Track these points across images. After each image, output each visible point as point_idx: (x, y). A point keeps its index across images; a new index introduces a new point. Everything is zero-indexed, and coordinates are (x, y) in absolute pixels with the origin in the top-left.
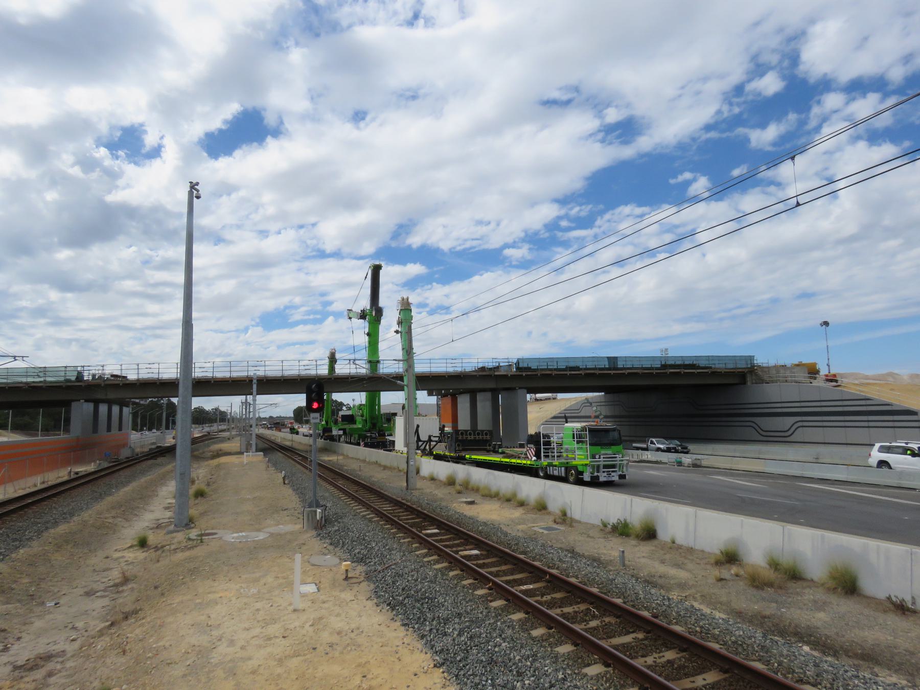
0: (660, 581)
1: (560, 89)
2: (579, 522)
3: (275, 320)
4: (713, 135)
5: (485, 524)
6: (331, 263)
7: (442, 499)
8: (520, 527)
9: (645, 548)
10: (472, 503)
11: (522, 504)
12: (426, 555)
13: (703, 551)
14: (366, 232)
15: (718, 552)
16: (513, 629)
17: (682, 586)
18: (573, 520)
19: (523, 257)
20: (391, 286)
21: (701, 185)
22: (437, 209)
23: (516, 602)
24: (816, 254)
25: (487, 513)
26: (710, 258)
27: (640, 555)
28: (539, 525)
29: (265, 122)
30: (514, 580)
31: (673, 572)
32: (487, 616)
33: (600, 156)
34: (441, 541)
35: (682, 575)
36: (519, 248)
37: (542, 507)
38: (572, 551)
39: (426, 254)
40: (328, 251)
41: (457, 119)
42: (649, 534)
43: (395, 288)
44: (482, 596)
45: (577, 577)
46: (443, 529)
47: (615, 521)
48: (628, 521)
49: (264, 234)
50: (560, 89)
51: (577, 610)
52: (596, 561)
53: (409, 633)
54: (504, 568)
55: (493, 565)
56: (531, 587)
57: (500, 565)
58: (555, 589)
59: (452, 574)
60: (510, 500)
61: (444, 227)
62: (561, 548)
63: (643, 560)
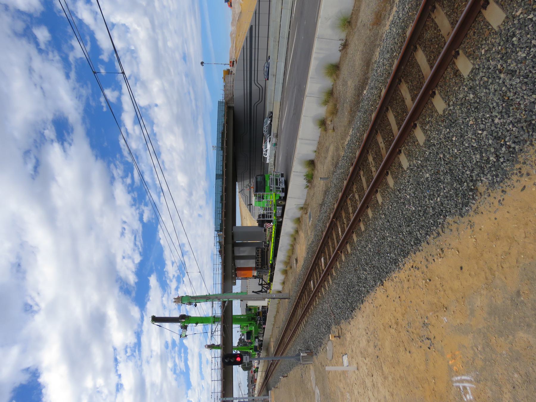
0: (335, 160)
1: (25, 163)
2: (306, 200)
3: (183, 376)
4: (73, 75)
5: (308, 253)
6: (144, 339)
7: (295, 278)
8: (309, 233)
9: (319, 166)
10: (296, 260)
11: (297, 232)
12: (325, 289)
13: (320, 137)
14: (123, 312)
15: (320, 129)
17: (337, 149)
19: (150, 211)
20: (164, 299)
21: (111, 95)
22: (110, 263)
23: (347, 239)
24: (160, 44)
25: (302, 252)
26: (159, 101)
27: (322, 169)
28: (308, 223)
29: (24, 382)
30: (336, 239)
31: (330, 153)
32: (355, 255)
33: (80, 145)
34: (317, 279)
35: (332, 148)
36: (143, 211)
37: (298, 221)
38: (322, 205)
39: (142, 272)
41: (40, 236)
42: (312, 163)
43: (166, 295)
44: (345, 257)
47: (305, 181)
49: (119, 387)
50: (25, 163)
53: (366, 300)
54: (330, 244)
55: (329, 250)
57: (329, 246)
59: (334, 274)
60: (295, 237)
61: (124, 258)
62: (320, 211)
63: (325, 168)
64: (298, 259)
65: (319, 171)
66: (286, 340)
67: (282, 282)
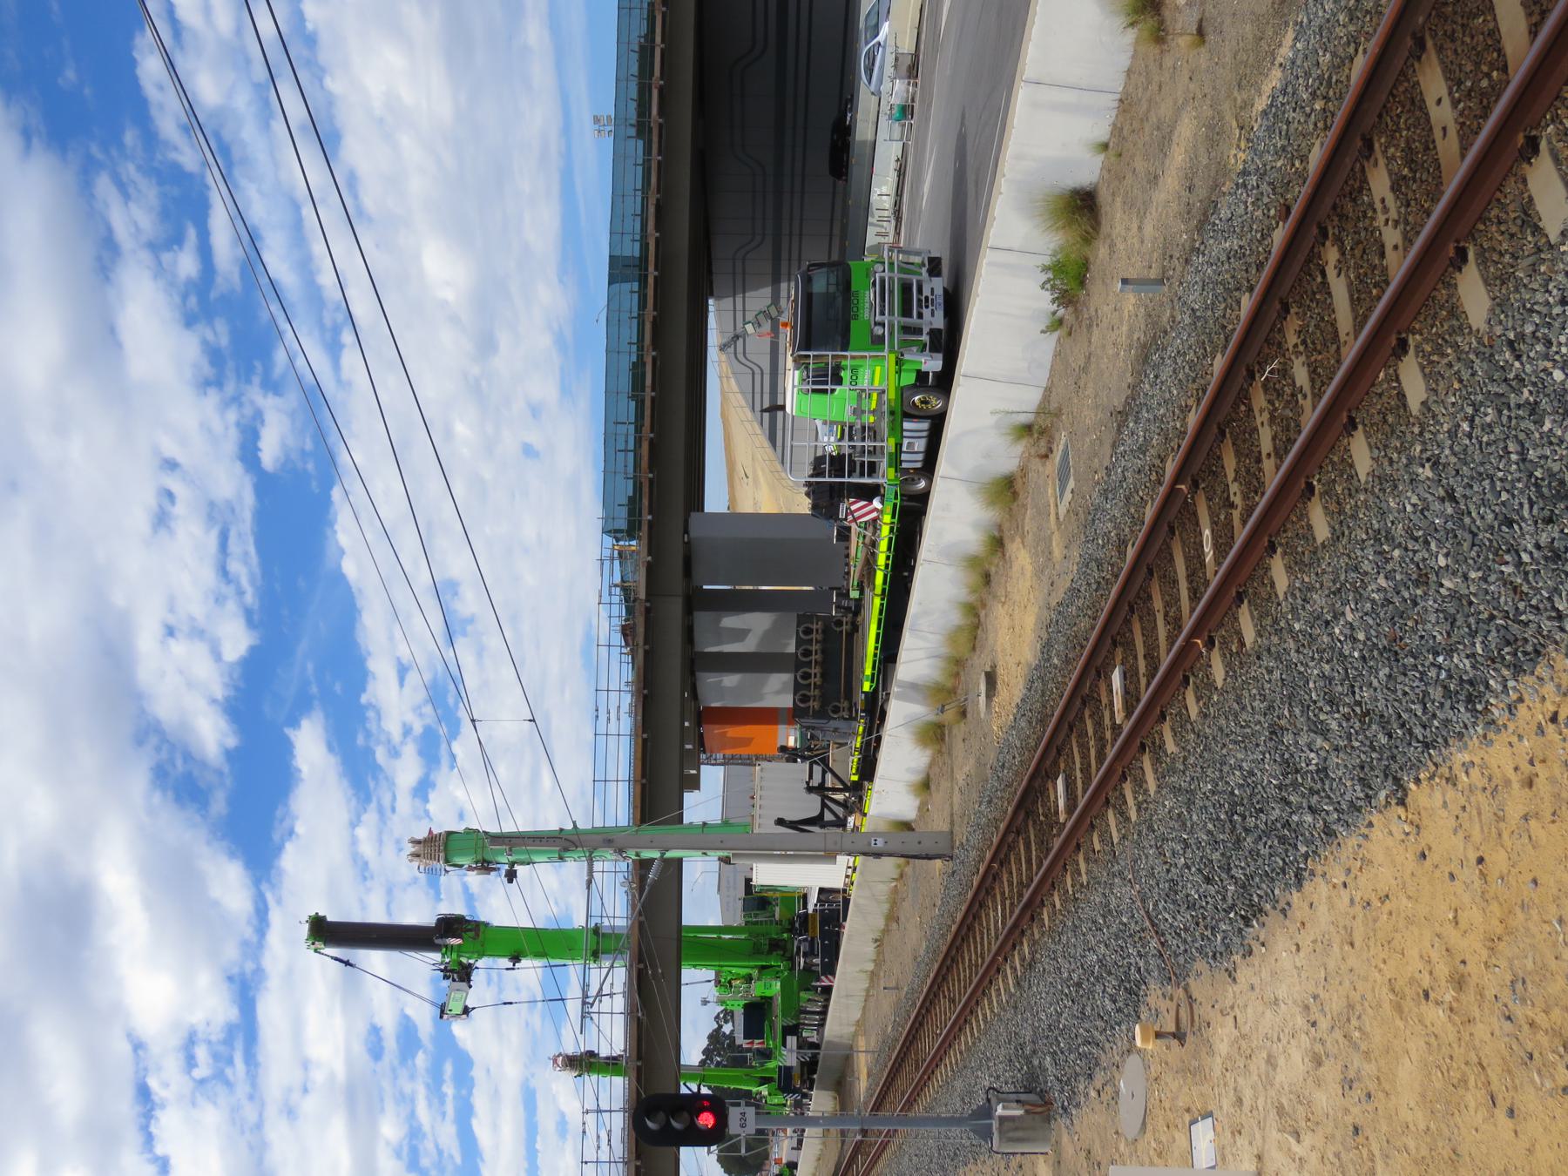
0: (1202, 191)
2: (1048, 391)
5: (1047, 646)
6: (270, 1009)
7: (980, 763)
8: (1057, 552)
9: (1116, 219)
10: (991, 679)
11: (997, 543)
12: (1123, 815)
13: (1129, 72)
14: (174, 885)
15: (1131, 35)
16: (1311, 589)
17: (1213, 134)
18: (1042, 410)
19: (292, 415)
20: (361, 832)
23: (1242, 580)
25: (1018, 639)
27: (1135, 237)
28: (1055, 501)
30: (1191, 577)
31: (1178, 157)
32: (1278, 658)
34: (1086, 770)
35: (1186, 129)
36: (258, 416)
37: (1006, 490)
38: (1122, 416)
39: (257, 699)
40: (233, 1014)
42: (1081, 207)
43: (371, 817)
44: (1229, 666)
45: (1186, 409)
46: (1055, 763)
47: (1048, 296)
48: (1047, 261)
51: (1266, 415)
52: (1146, 354)
53: (1319, 869)
54: (1158, 604)
56: (1207, 532)
57: (1151, 613)
58: (1214, 470)
59: (1171, 747)
60: (986, 571)
61: (170, 632)
62: (1114, 446)
63: (1149, 229)
64: (1000, 671)
65: (1120, 246)
66: (928, 1045)
67: (917, 778)
